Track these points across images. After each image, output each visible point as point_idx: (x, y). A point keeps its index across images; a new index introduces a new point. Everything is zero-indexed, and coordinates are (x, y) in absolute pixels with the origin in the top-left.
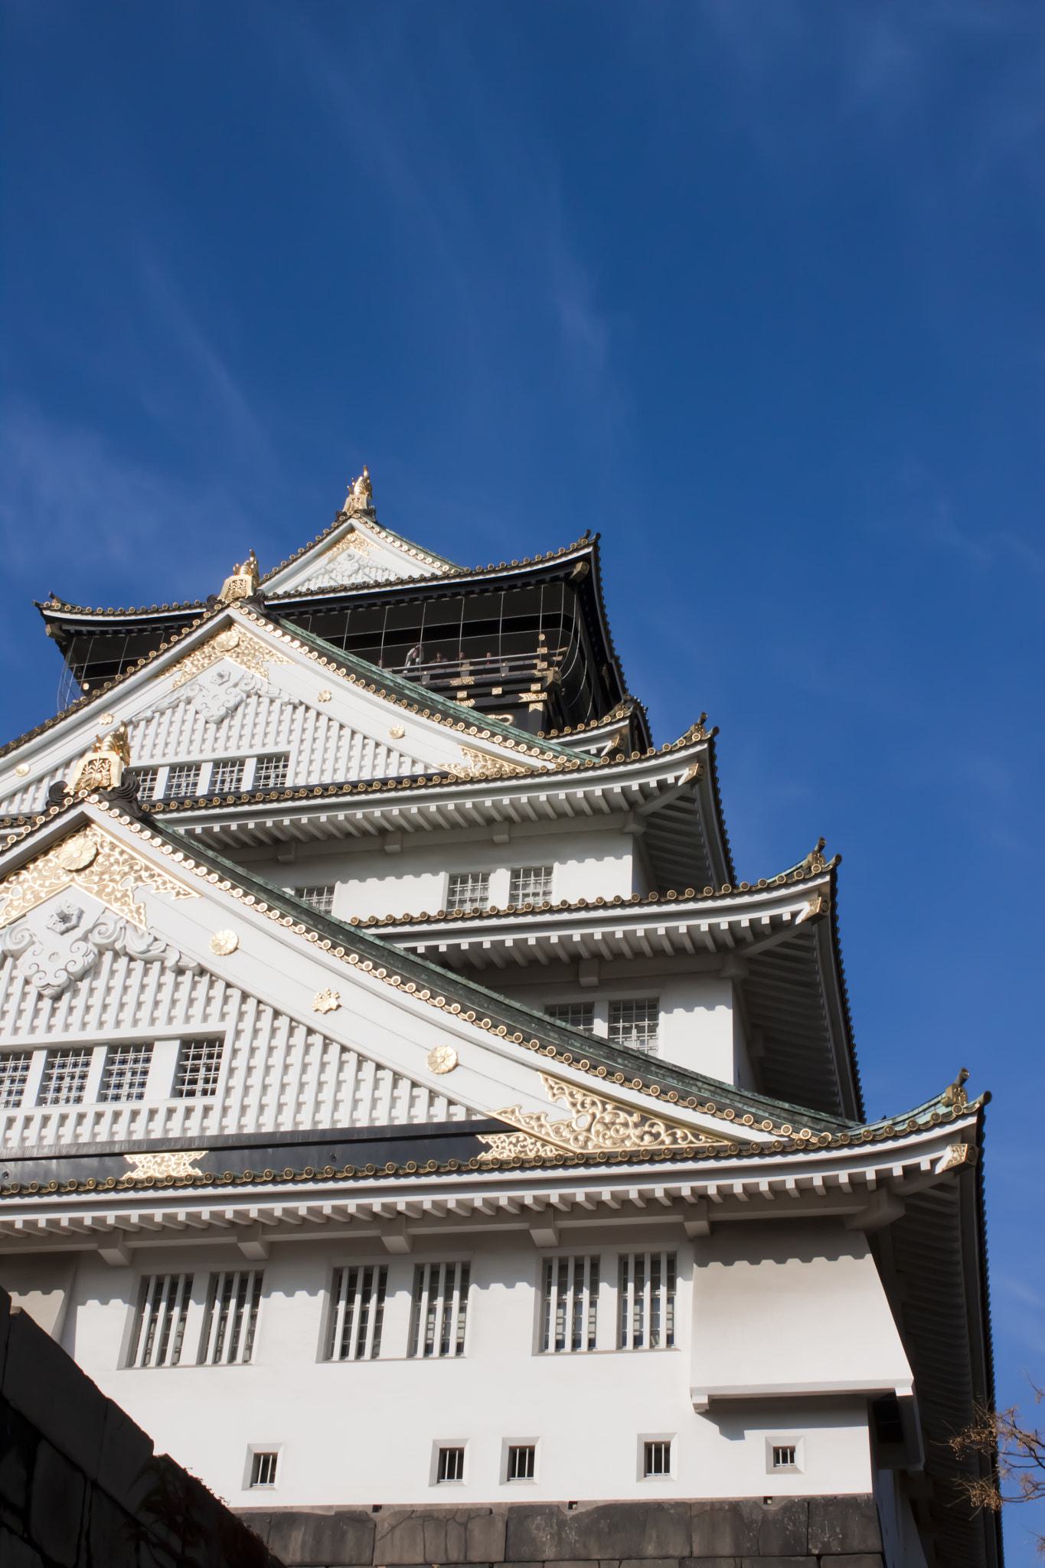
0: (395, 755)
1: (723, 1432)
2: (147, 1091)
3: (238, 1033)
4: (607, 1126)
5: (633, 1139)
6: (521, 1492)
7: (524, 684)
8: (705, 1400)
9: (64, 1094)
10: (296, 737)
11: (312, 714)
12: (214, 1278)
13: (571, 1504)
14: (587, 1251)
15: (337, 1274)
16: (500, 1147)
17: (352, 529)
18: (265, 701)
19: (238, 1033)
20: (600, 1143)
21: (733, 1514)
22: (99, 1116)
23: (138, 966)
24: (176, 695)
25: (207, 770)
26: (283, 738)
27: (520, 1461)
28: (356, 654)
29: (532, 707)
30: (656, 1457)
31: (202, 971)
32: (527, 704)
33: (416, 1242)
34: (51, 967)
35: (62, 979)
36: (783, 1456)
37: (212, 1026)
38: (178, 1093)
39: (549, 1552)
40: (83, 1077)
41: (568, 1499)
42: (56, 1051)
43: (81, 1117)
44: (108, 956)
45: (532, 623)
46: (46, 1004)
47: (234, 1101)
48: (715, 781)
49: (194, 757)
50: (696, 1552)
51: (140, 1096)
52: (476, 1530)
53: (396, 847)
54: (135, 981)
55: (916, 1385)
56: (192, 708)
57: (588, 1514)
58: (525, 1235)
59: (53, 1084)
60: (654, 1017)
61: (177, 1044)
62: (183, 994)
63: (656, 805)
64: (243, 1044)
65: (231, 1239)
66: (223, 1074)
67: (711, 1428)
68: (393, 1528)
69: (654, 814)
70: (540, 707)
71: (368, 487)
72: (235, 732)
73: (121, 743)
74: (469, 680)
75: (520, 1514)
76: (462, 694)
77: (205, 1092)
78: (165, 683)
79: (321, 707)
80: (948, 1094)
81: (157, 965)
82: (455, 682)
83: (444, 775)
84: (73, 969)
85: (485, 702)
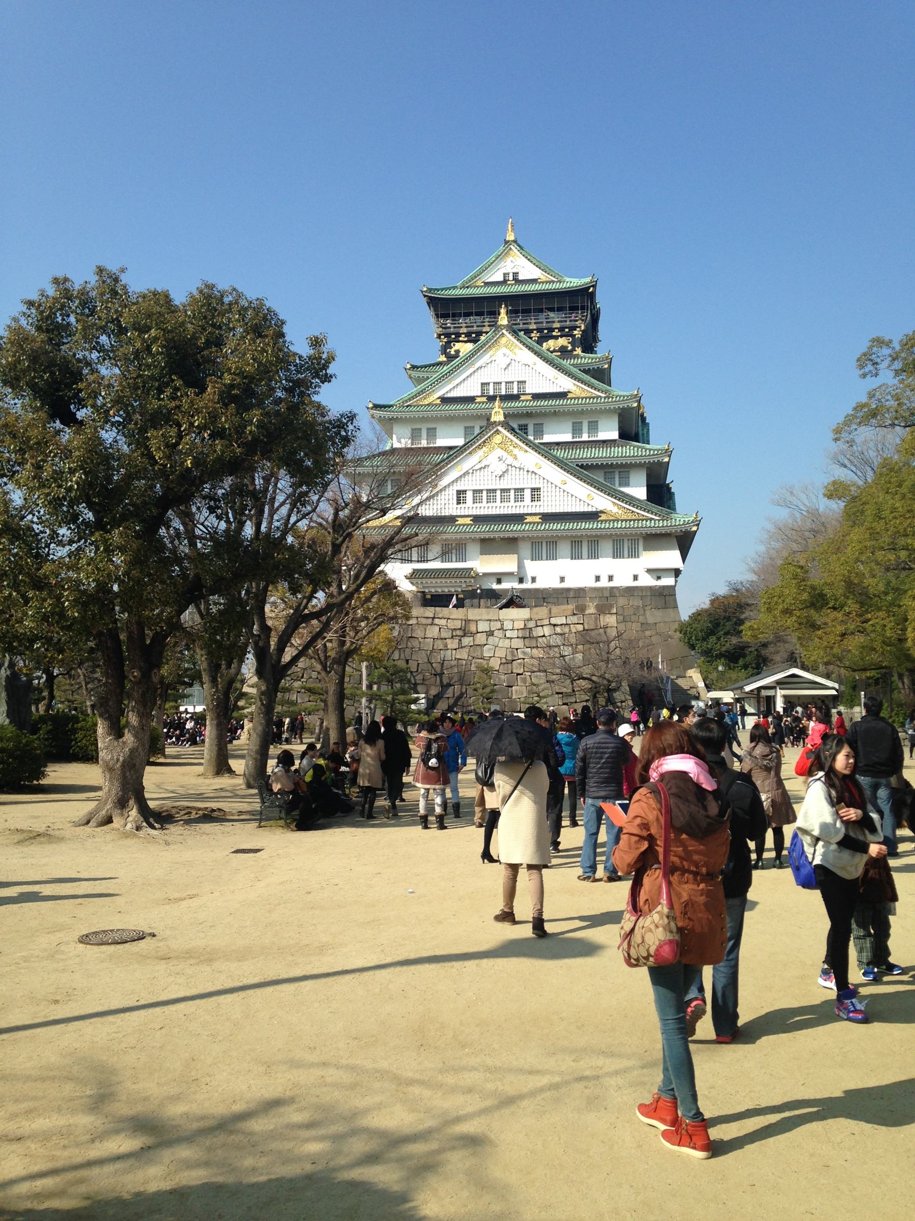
6: (612, 584)
7: (575, 328)
21: (650, 588)
25: (503, 385)
27: (611, 578)
30: (636, 578)
42: (503, 490)
45: (576, 308)
64: (545, 489)
74: (557, 325)
75: (612, 588)
78: (488, 355)
85: (564, 333)
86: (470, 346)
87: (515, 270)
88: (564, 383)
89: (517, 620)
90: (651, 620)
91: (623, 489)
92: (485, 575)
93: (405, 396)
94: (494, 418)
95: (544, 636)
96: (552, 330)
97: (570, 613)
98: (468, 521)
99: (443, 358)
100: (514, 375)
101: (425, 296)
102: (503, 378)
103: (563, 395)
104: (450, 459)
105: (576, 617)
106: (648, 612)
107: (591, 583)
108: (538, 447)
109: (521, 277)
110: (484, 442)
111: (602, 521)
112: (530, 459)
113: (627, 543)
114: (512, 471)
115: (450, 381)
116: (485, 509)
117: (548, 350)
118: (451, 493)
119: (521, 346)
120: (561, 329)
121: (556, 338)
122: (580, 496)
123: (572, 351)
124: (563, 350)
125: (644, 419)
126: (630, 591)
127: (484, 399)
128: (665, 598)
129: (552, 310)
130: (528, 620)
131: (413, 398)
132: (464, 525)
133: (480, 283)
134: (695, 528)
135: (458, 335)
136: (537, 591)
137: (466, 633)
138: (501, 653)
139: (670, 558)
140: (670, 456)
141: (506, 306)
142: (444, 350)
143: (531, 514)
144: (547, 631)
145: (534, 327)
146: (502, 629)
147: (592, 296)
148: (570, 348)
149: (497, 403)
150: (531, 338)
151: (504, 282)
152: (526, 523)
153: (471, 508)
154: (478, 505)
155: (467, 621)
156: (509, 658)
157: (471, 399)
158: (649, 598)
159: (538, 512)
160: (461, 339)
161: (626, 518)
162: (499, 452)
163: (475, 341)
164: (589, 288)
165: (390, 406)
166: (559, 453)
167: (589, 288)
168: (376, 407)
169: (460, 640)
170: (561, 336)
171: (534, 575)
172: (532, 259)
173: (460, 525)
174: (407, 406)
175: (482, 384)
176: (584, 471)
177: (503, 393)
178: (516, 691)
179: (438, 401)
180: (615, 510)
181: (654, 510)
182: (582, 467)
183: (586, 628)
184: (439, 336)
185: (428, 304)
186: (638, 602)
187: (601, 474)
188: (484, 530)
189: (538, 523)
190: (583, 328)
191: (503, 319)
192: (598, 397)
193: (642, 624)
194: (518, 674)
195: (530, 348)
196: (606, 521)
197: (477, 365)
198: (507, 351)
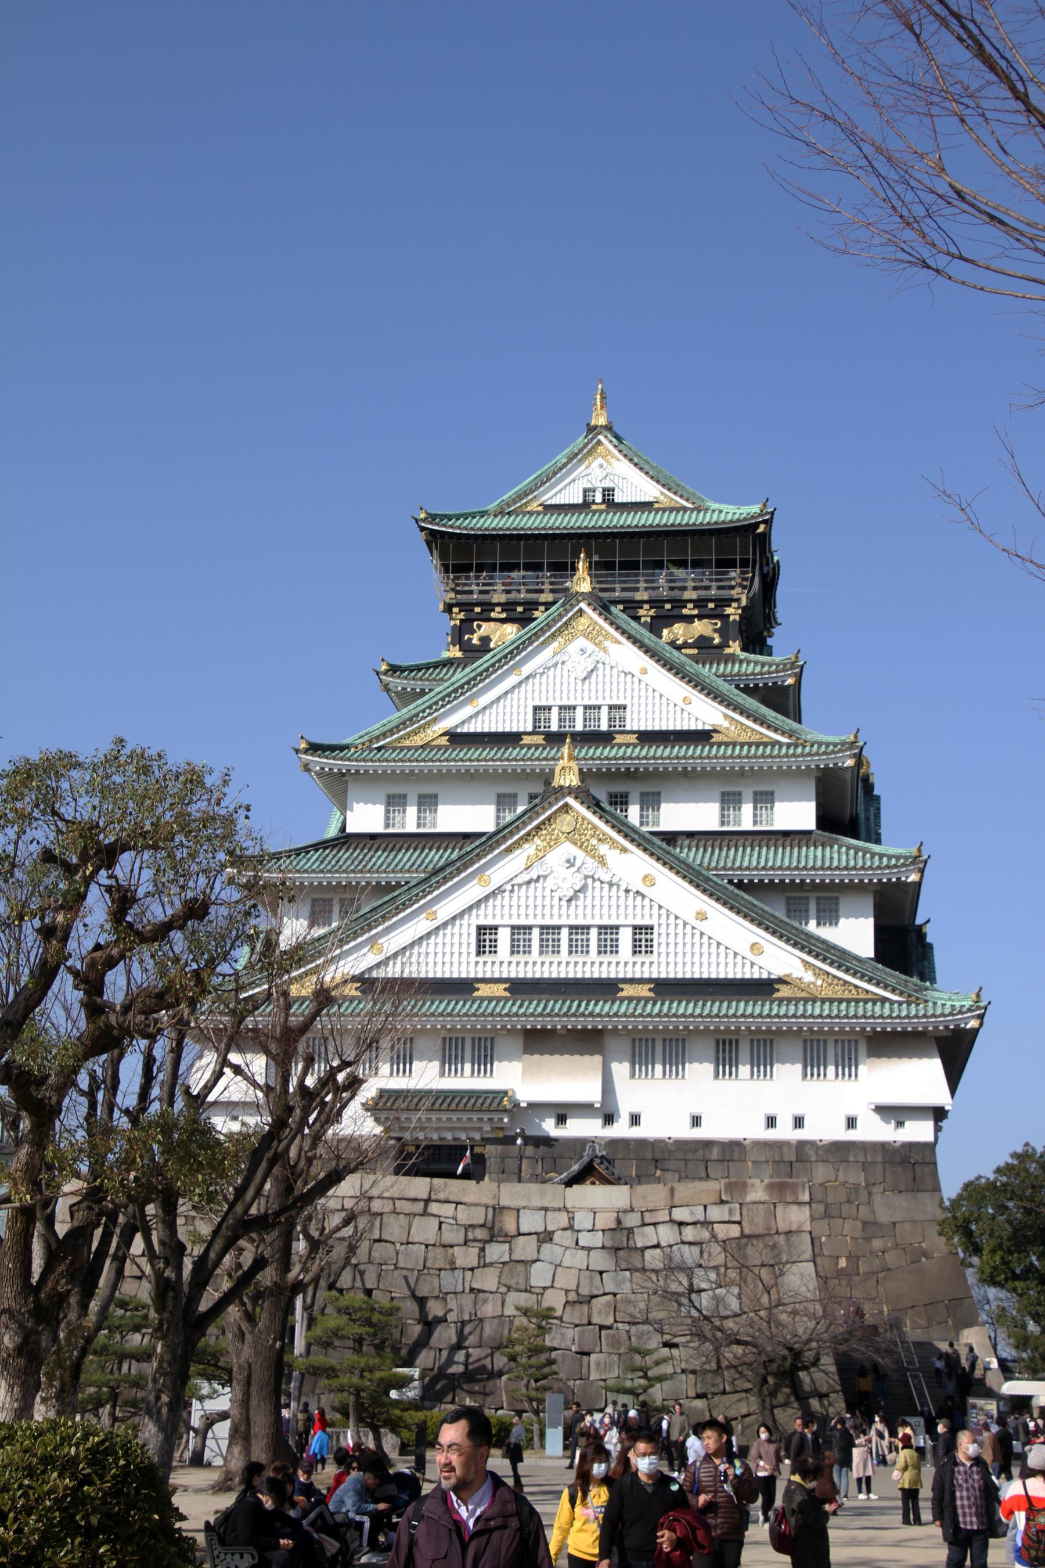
1: (883, 1119)
2: (620, 949)
5: (840, 992)
7: (728, 602)
11: (636, 679)
12: (664, 1040)
15: (718, 1041)
18: (608, 668)
20: (828, 993)
23: (606, 886)
24: (555, 659)
25: (580, 711)
26: (621, 694)
27: (799, 1122)
29: (731, 618)
30: (851, 1123)
31: (637, 892)
32: (728, 616)
35: (571, 893)
36: (900, 1124)
37: (646, 922)
39: (813, 1158)
40: (588, 940)
44: (590, 881)
46: (564, 903)
47: (663, 958)
49: (572, 703)
52: (785, 1150)
56: (566, 667)
60: (837, 904)
64: (663, 930)
66: (655, 943)
67: (876, 1117)
70: (737, 618)
75: (802, 1144)
76: (690, 605)
81: (615, 888)
84: (577, 888)
85: (704, 611)
86: (511, 631)
87: (607, 484)
88: (706, 714)
89: (604, 1210)
90: (884, 1216)
91: (826, 933)
92: (533, 1106)
93: (376, 728)
94: (559, 781)
95: (657, 1246)
96: (682, 603)
97: (714, 1198)
98: (499, 990)
99: (456, 653)
100: (602, 693)
101: (422, 529)
103: (702, 737)
104: (465, 862)
105: (726, 1207)
106: (877, 1199)
108: (649, 841)
109: (618, 498)
110: (538, 828)
111: (781, 1000)
112: (633, 865)
113: (831, 1047)
114: (595, 890)
115: (470, 700)
116: (537, 966)
117: (672, 644)
118: (464, 930)
119: (617, 635)
120: (700, 603)
121: (689, 619)
122: (732, 944)
123: (724, 645)
124: (703, 643)
125: (868, 787)
126: (839, 1150)
127: (539, 739)
128: (913, 1165)
129: (681, 564)
130: (625, 1212)
131: (391, 732)
132: (490, 999)
133: (534, 506)
134: (973, 1024)
135: (488, 607)
136: (642, 1143)
137: (494, 1233)
138: (566, 1280)
140: (922, 871)
141: (588, 555)
142: (459, 636)
143: (632, 981)
144: (666, 1234)
145: (646, 598)
146: (571, 1227)
147: (764, 540)
148: (717, 641)
149: (565, 750)
150: (637, 618)
151: (585, 506)
152: (622, 1000)
153: (505, 963)
154: (522, 958)
155: (498, 1210)
156: (585, 1291)
157: (511, 739)
158: (880, 1167)
159: (646, 975)
160: (493, 615)
161: (830, 995)
162: (567, 849)
163: (524, 620)
164: (756, 525)
165: (342, 748)
166: (692, 855)
167: (756, 525)
168: (314, 748)
169: (483, 1250)
170: (700, 617)
171: (635, 1110)
172: (642, 464)
173: (482, 999)
174: (379, 749)
175: (535, 708)
176: (746, 896)
177: (579, 727)
178: (598, 1364)
179: (444, 741)
180: (808, 977)
181: (891, 981)
182: (740, 885)
183: (747, 1231)
184: (448, 608)
185: (429, 544)
186: (855, 1177)
187: (778, 901)
188: (534, 1012)
189: (647, 1000)
190: (744, 603)
191: (583, 583)
192: (774, 743)
193: (865, 1224)
194: (602, 1327)
195: (635, 641)
196: (789, 1000)
197: (526, 669)
198: (590, 647)
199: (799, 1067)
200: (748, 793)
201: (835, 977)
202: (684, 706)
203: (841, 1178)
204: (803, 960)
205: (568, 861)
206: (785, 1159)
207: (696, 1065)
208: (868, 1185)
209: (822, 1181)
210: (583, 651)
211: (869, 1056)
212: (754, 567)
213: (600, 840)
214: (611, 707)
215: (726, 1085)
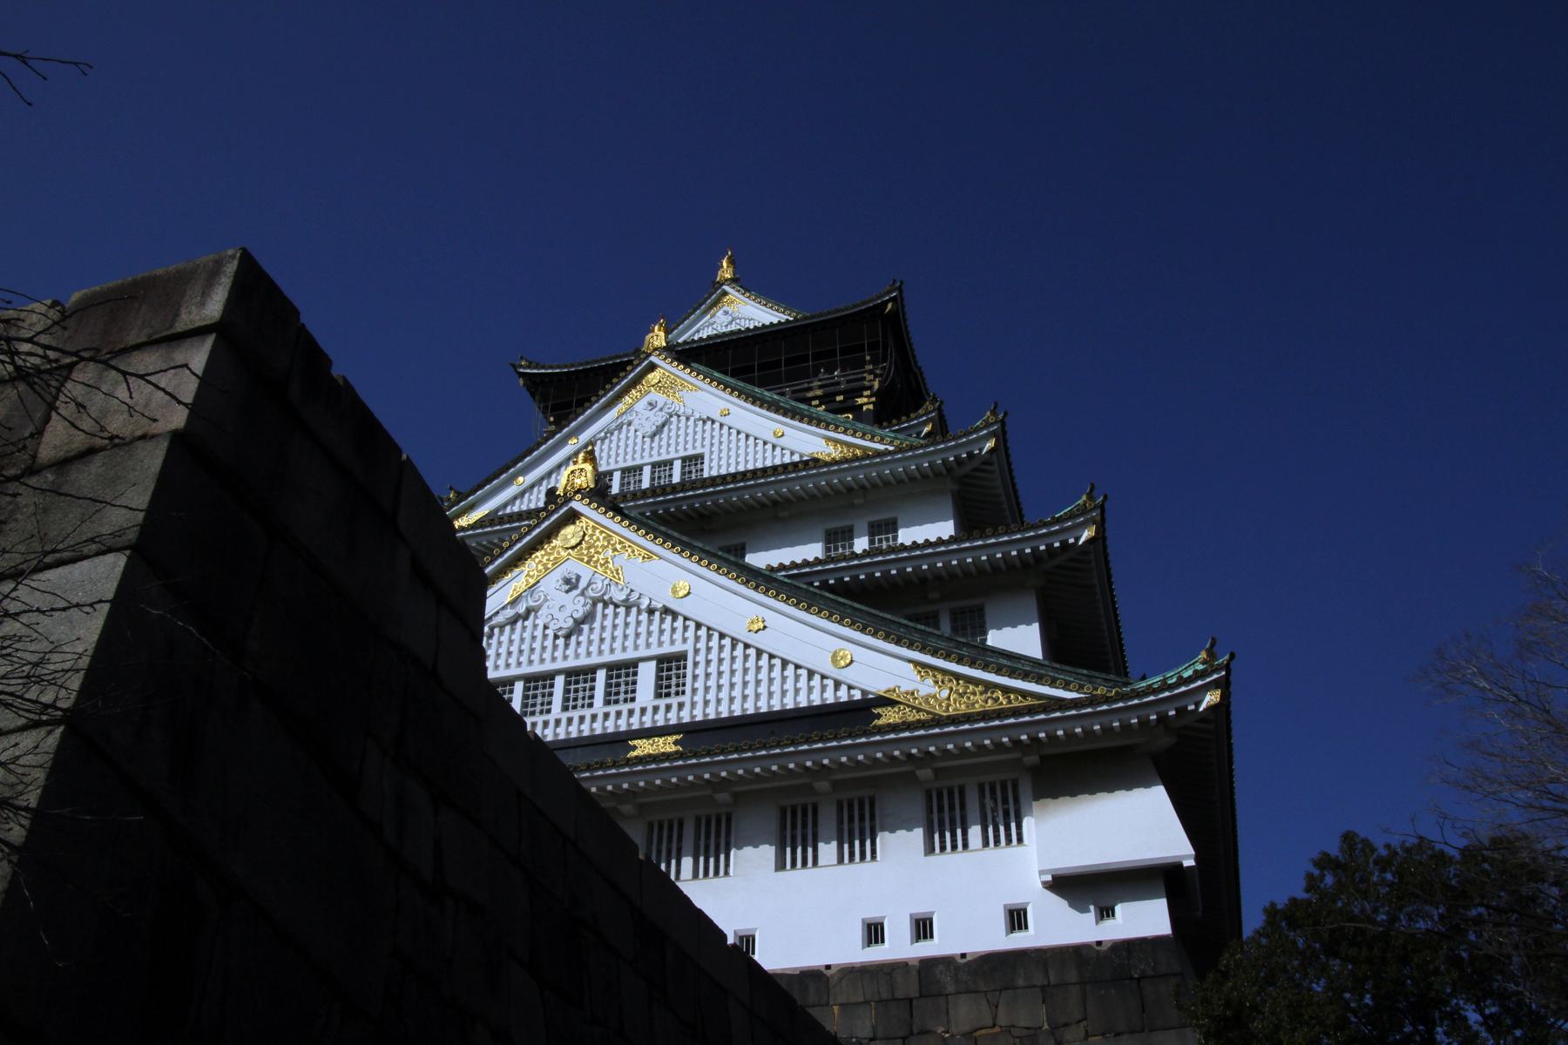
0: (778, 450)
2: (638, 695)
3: (697, 651)
4: (961, 695)
5: (980, 703)
6: (926, 949)
8: (1049, 878)
9: (580, 702)
10: (707, 442)
11: (717, 425)
12: (698, 820)
13: (963, 956)
14: (956, 782)
16: (889, 716)
17: (725, 293)
18: (683, 419)
19: (697, 651)
21: (1077, 955)
22: (606, 716)
23: (622, 610)
25: (647, 471)
26: (698, 444)
27: (922, 928)
28: (744, 380)
30: (1017, 918)
31: (666, 611)
33: (836, 785)
34: (560, 616)
35: (570, 622)
36: (1106, 912)
37: (678, 647)
38: (658, 695)
39: (951, 988)
40: (592, 689)
41: (959, 951)
42: (572, 674)
43: (594, 717)
44: (600, 606)
46: (561, 642)
47: (699, 698)
48: (1006, 449)
49: (638, 462)
50: (1053, 980)
51: (633, 700)
53: (786, 514)
54: (620, 621)
55: (1197, 858)
56: (632, 428)
57: (975, 961)
58: (912, 774)
59: (572, 695)
61: (654, 663)
62: (655, 627)
63: (968, 468)
64: (701, 658)
65: (708, 792)
66: (689, 679)
68: (841, 980)
69: (966, 476)
71: (732, 262)
72: (664, 443)
73: (591, 458)
74: (819, 392)
75: (928, 964)
76: (815, 402)
77: (677, 693)
78: (613, 413)
79: (723, 420)
80: (1203, 655)
81: (634, 610)
82: (810, 394)
83: (816, 460)
84: (576, 615)
85: (834, 406)
101: (521, 375)
102: (645, 456)
107: (850, 951)
111: (881, 730)
114: (606, 618)
126: (995, 970)
139: (1140, 824)
177: (646, 484)
180: (926, 687)
186: (1029, 1014)
199: (918, 833)
200: (861, 524)
201: (970, 680)
202: (774, 441)
203: (1003, 1020)
204: (916, 663)
205: (567, 581)
206: (899, 995)
207: (748, 851)
208: (1054, 1028)
209: (966, 1028)
210: (652, 405)
211: (1038, 796)
212: (885, 349)
213: (615, 550)
214: (684, 459)
215: (797, 878)
